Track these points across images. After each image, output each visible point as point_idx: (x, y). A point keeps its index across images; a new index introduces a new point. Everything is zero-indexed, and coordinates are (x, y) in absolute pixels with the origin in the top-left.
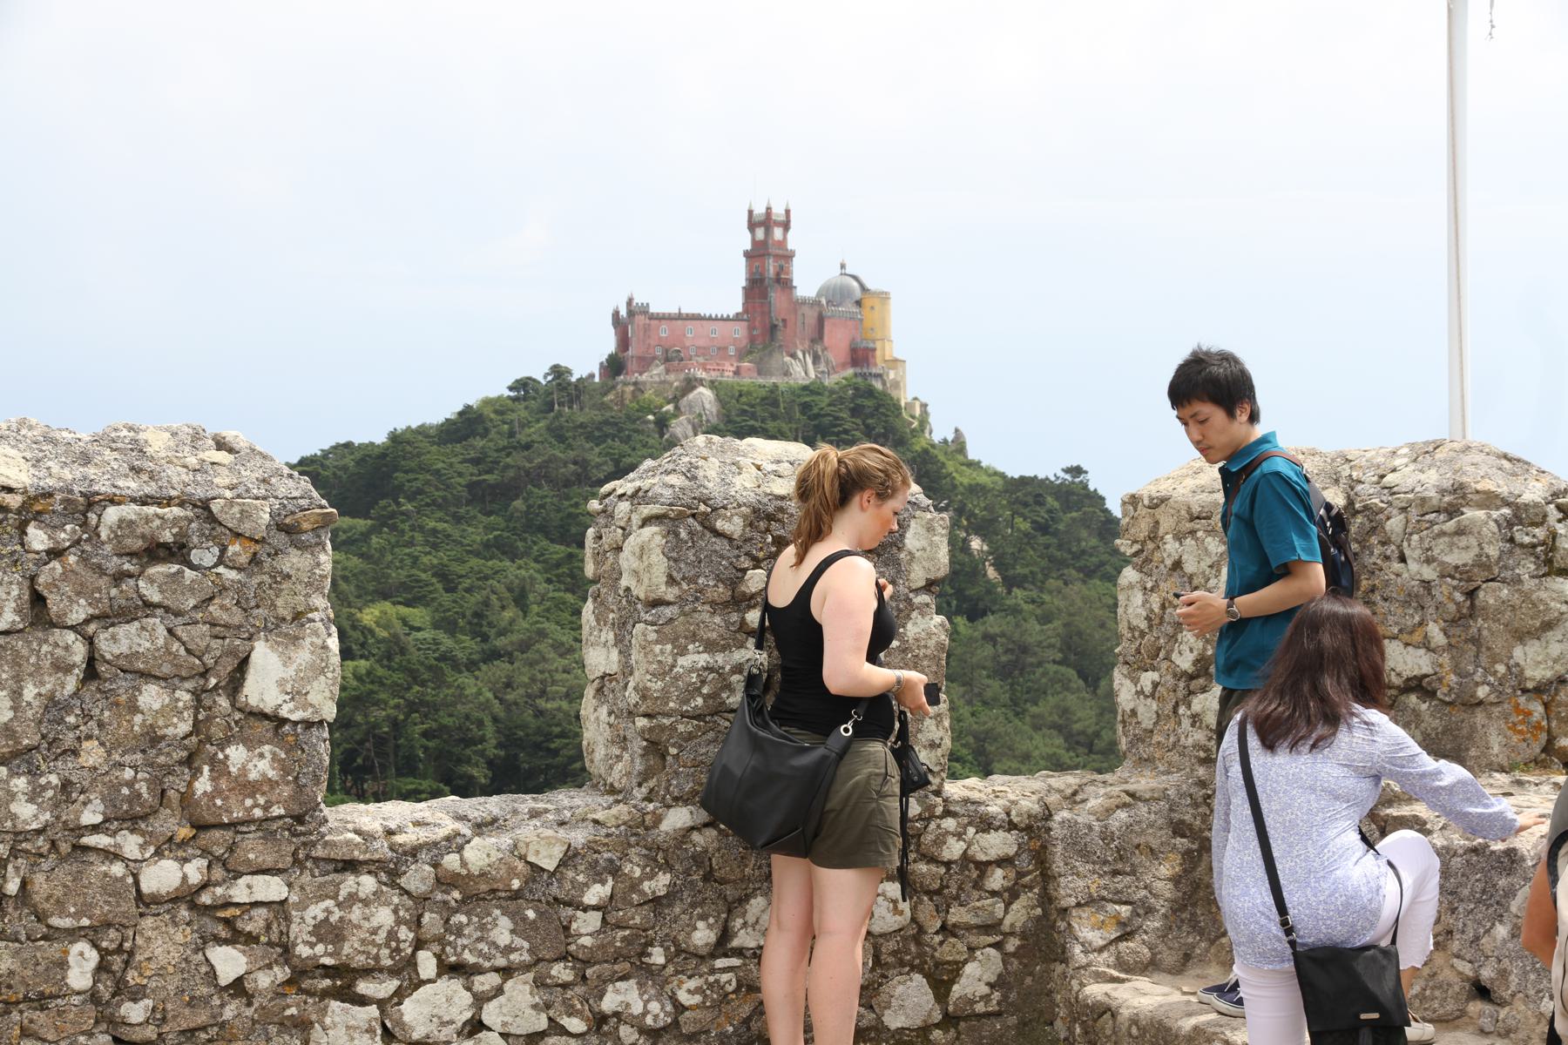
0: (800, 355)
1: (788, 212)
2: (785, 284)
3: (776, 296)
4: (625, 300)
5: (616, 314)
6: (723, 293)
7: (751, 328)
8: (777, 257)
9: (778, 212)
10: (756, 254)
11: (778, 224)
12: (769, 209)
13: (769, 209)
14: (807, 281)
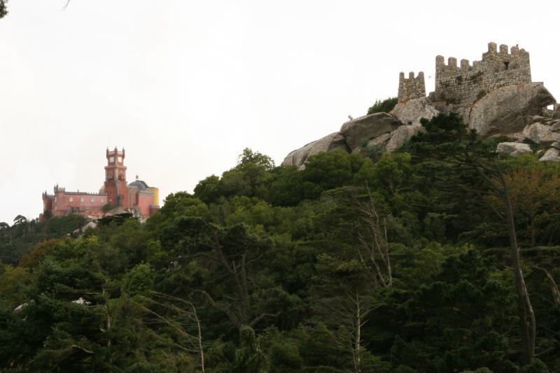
1: (124, 151)
2: (122, 178)
3: (118, 185)
7: (109, 199)
8: (120, 169)
9: (120, 150)
10: (110, 169)
11: (120, 156)
12: (116, 150)
13: (116, 150)
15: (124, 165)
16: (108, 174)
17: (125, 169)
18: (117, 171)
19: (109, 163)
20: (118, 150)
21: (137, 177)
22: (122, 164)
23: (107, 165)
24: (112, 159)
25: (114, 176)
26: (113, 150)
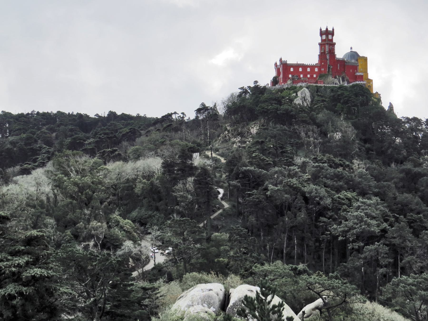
0: (338, 77)
2: (332, 52)
4: (279, 59)
5: (276, 64)
9: (330, 29)
12: (327, 29)
13: (327, 29)
14: (340, 53)
15: (334, 41)
16: (321, 49)
17: (335, 44)
18: (327, 47)
19: (322, 40)
20: (329, 29)
21: (351, 48)
22: (332, 40)
23: (320, 41)
24: (324, 37)
25: (325, 50)
26: (325, 29)
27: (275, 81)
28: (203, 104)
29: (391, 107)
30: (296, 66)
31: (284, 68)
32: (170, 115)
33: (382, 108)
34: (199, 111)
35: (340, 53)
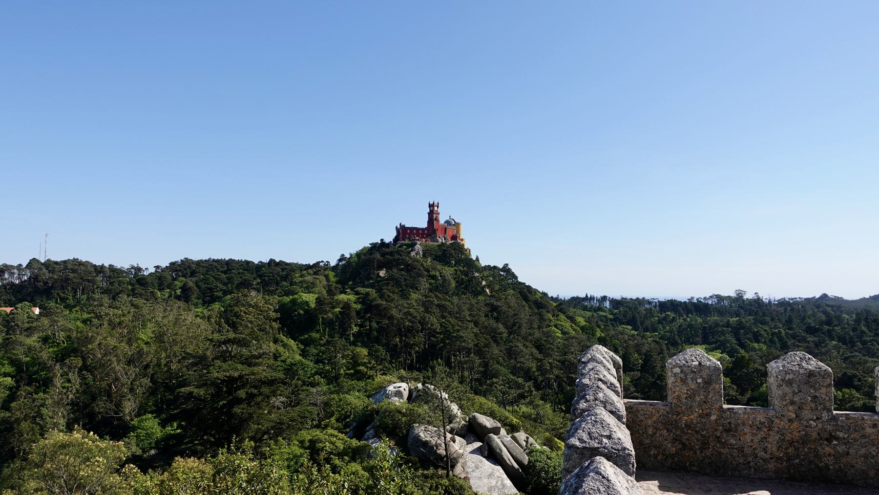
2: (437, 220)
6: (423, 224)
9: (436, 203)
10: (431, 214)
14: (442, 221)
27: (396, 239)
28: (343, 255)
29: (477, 259)
30: (412, 229)
31: (403, 232)
32: (318, 263)
33: (471, 259)
34: (340, 260)
35: (442, 221)
